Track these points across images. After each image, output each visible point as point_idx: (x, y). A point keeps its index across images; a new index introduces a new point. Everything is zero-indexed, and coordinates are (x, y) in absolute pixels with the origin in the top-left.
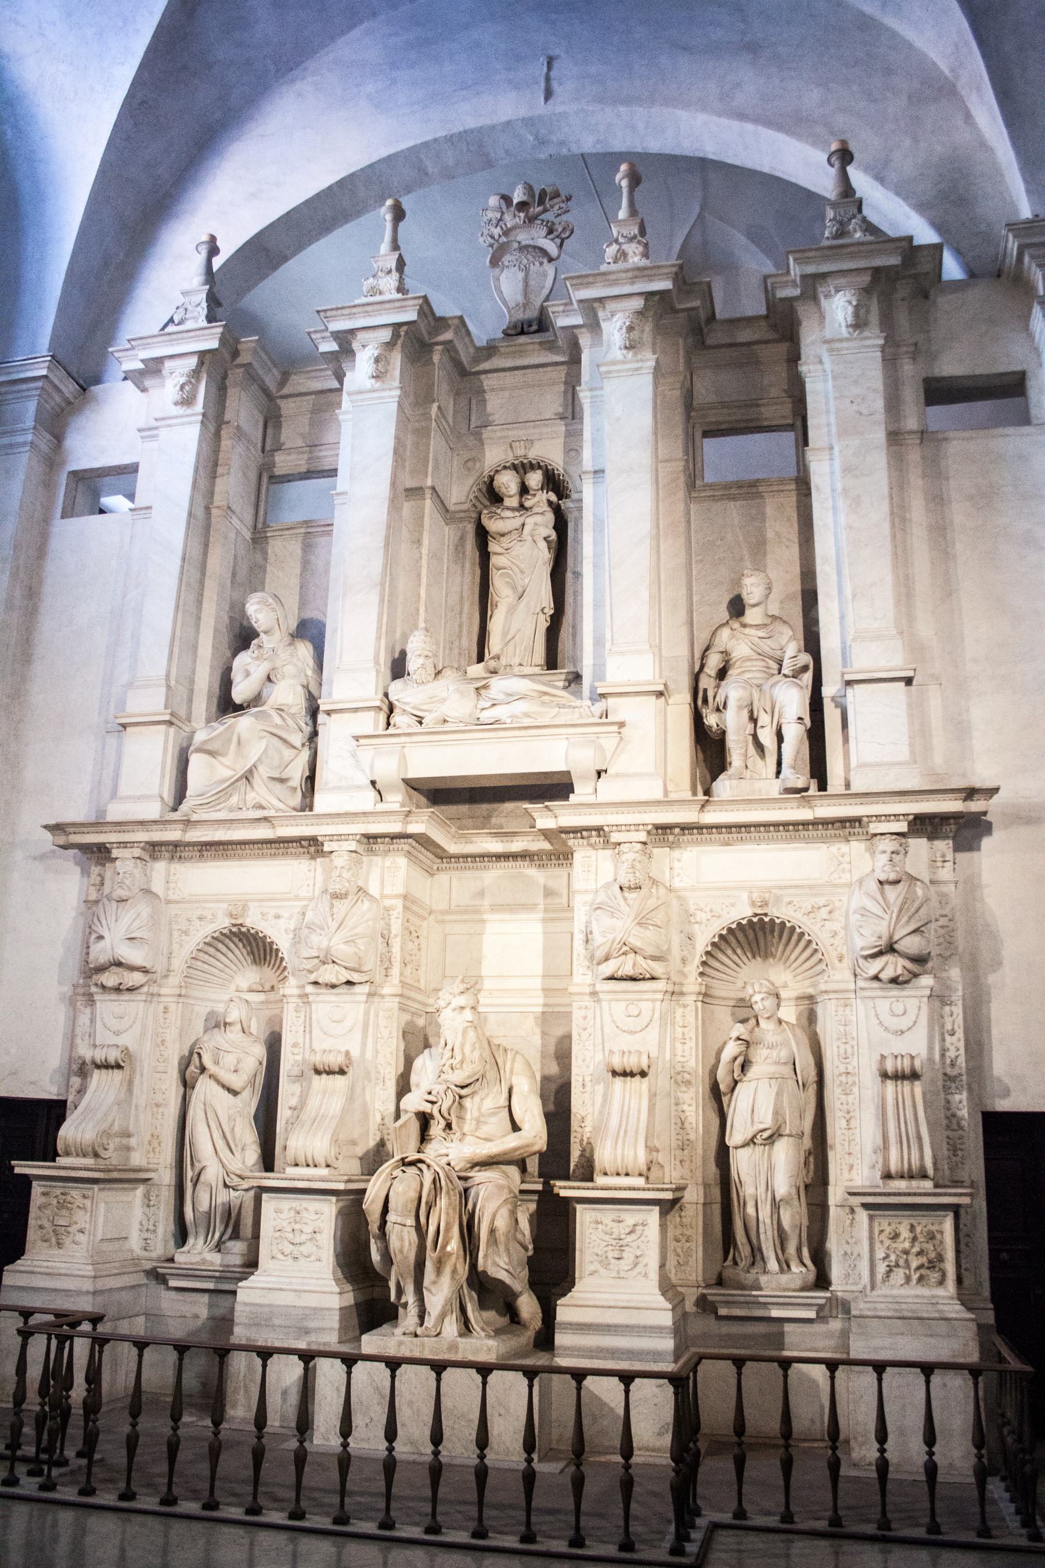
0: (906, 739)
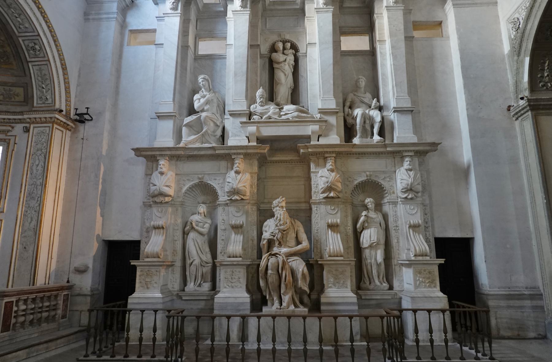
0: (412, 128)
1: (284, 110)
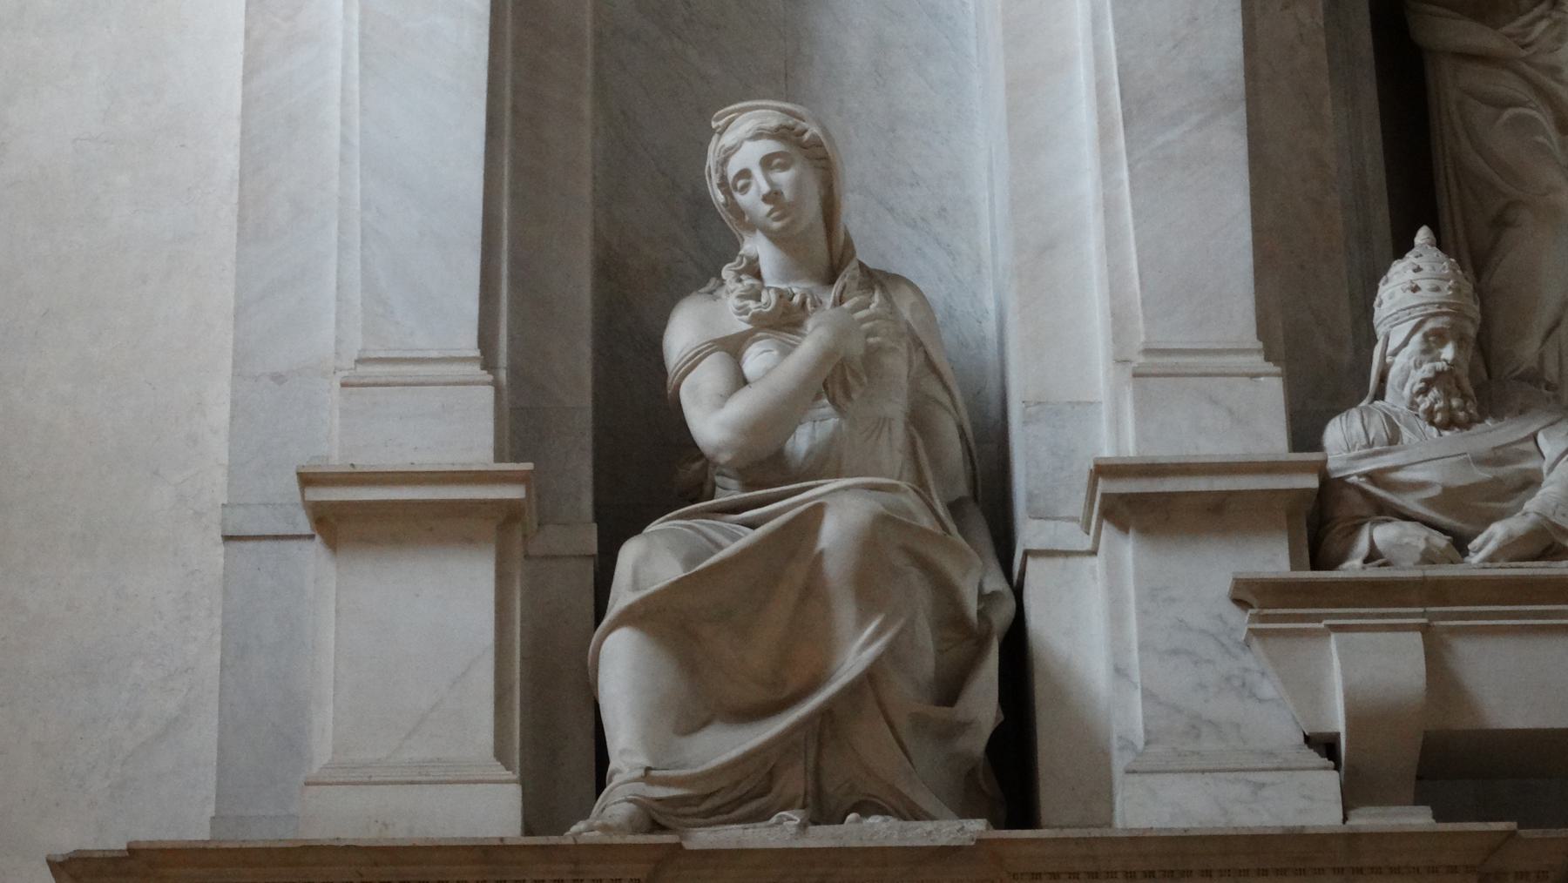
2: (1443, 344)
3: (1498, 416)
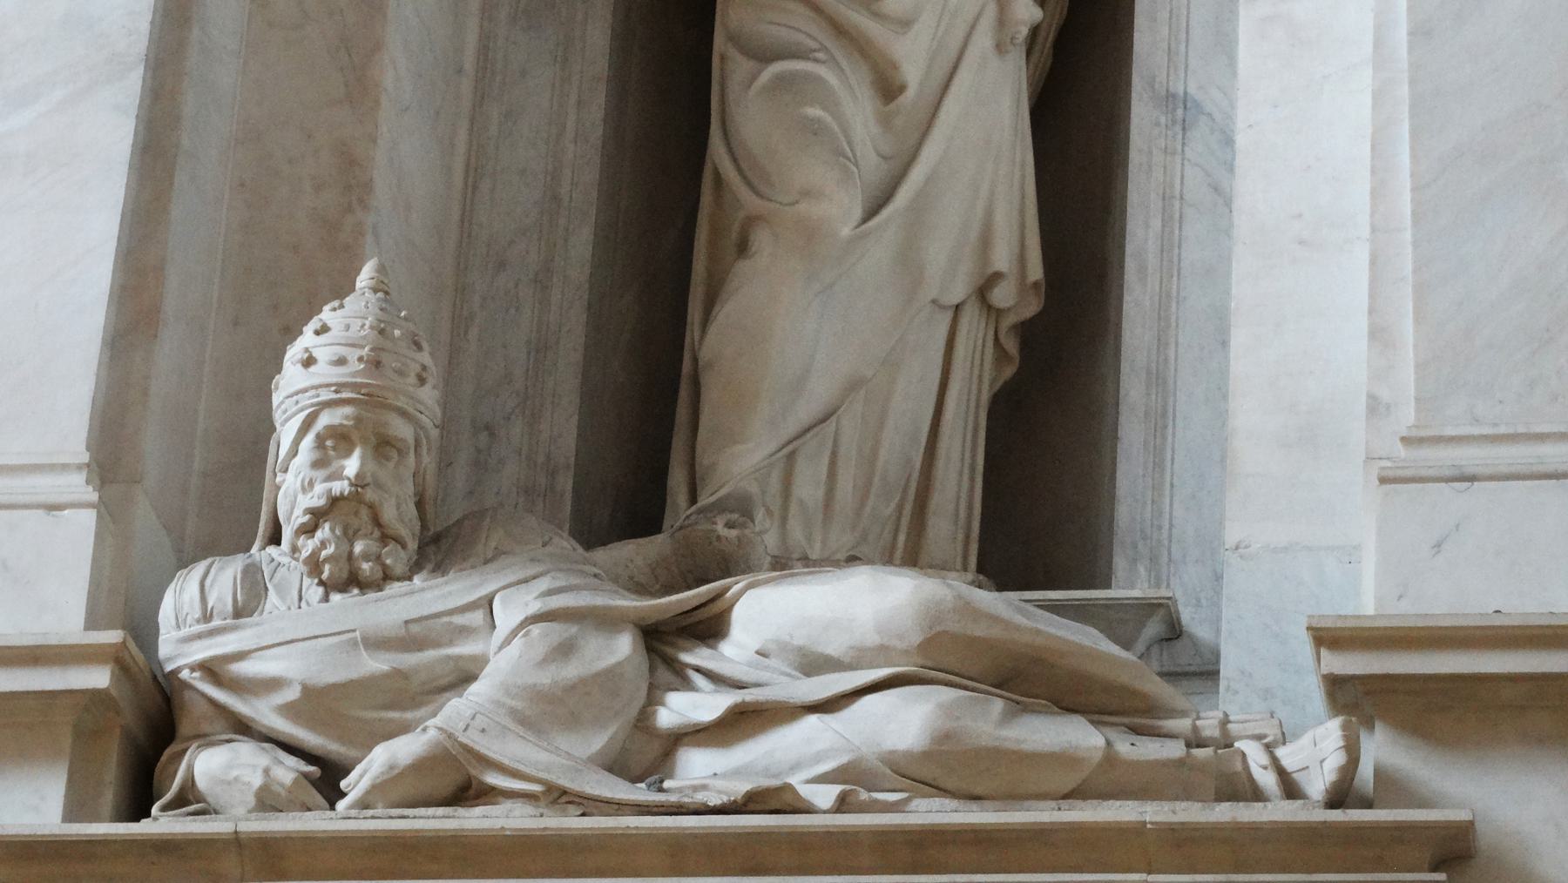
1: (736, 650)
2: (348, 454)
3: (440, 568)
